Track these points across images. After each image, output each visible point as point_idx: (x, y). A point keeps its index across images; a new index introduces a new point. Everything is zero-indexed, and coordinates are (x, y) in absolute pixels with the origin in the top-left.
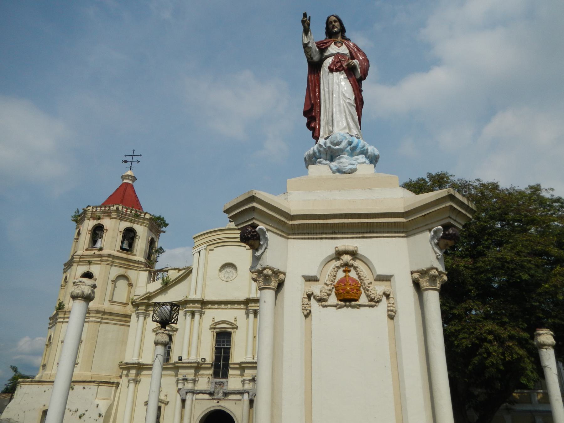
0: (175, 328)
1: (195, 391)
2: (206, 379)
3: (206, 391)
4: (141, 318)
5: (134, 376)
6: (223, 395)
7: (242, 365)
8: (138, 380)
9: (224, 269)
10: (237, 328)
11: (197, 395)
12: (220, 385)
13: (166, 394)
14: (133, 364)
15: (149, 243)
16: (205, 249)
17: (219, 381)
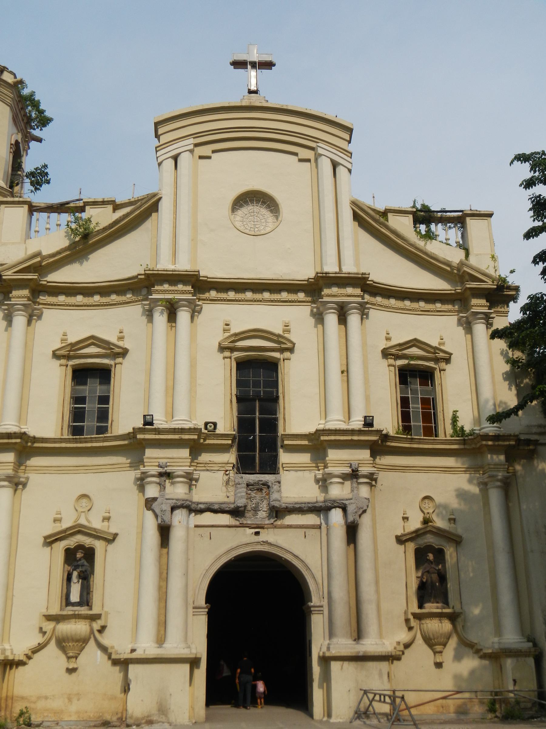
0: (119, 347)
1: (193, 506)
2: (220, 476)
3: (223, 506)
4: (20, 320)
5: (12, 467)
6: (270, 515)
7: (322, 438)
8: (22, 480)
9: (241, 206)
10: (291, 350)
11: (198, 516)
12: (258, 490)
13: (107, 515)
14: (9, 436)
15: (12, 151)
16: (191, 151)
17: (257, 479)
